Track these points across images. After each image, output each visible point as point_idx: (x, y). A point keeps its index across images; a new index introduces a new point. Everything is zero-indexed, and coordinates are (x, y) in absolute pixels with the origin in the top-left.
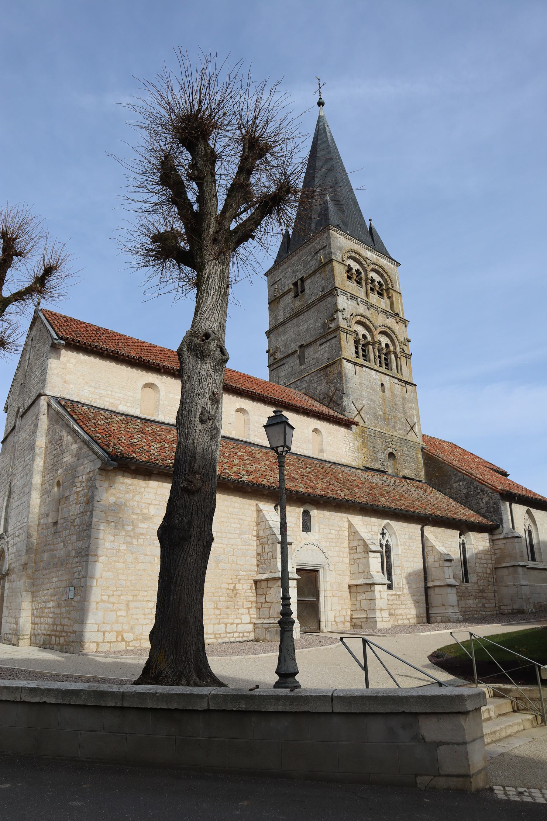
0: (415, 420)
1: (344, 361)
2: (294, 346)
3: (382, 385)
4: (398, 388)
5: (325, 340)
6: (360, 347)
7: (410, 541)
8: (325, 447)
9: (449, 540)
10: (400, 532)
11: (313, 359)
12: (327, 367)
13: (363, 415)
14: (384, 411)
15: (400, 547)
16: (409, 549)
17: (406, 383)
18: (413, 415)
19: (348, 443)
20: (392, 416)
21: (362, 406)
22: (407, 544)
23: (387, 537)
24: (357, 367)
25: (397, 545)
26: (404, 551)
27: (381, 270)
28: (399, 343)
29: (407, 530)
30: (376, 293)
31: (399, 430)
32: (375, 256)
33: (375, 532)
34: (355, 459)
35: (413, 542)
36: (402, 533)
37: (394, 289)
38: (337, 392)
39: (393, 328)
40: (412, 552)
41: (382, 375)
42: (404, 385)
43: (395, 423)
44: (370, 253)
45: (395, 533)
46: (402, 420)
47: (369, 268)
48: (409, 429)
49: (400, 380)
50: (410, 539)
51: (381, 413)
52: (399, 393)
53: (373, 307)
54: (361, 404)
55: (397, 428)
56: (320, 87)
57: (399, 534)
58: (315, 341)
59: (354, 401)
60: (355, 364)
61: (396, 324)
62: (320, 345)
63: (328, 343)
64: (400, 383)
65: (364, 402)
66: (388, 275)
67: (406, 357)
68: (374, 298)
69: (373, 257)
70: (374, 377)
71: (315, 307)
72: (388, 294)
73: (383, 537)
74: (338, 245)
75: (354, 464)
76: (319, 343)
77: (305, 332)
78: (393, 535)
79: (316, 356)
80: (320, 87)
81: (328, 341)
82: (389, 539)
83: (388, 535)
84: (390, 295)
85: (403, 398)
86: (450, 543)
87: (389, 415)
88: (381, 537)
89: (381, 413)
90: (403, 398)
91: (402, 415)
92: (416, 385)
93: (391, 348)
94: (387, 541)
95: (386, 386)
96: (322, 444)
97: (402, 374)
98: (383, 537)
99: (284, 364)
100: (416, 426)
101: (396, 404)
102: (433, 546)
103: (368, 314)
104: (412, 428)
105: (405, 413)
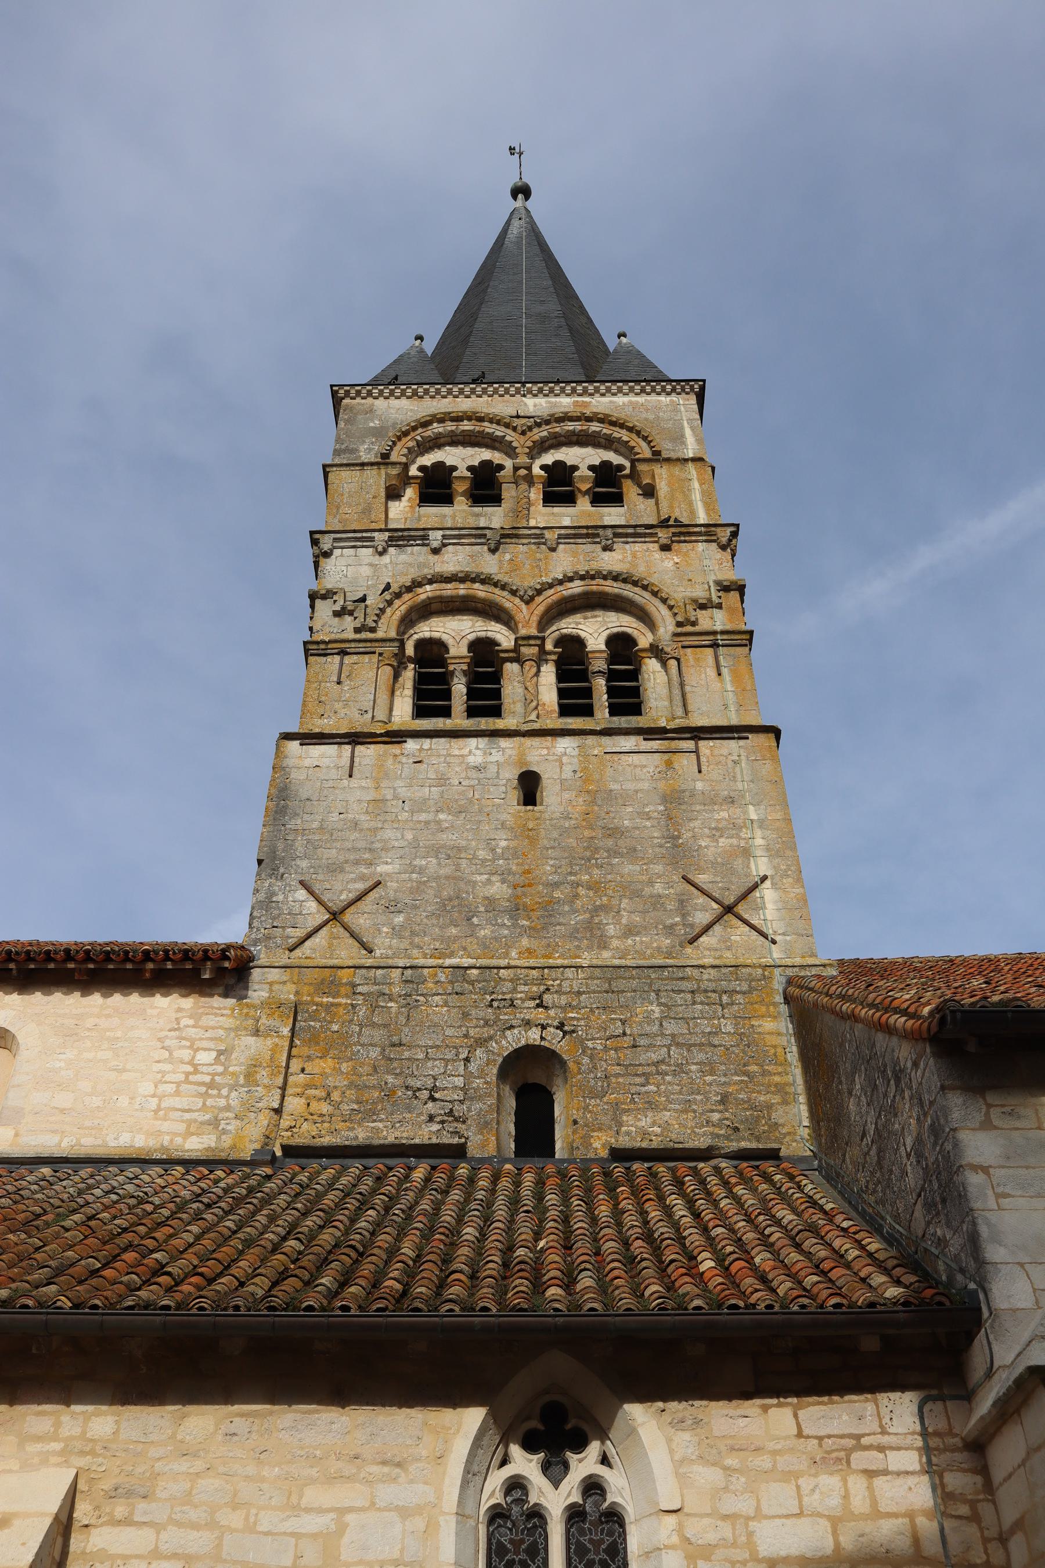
1: (294, 745)
9: (313, 1496)
19: (186, 1054)
27: (595, 427)
28: (671, 608)
34: (215, 1123)
37: (665, 454)
39: (639, 571)
43: (597, 910)
54: (362, 878)
55: (611, 930)
61: (658, 555)
64: (655, 745)
70: (476, 759)
75: (196, 1145)
86: (312, 1523)
87: (556, 885)
89: (498, 889)
101: (614, 832)
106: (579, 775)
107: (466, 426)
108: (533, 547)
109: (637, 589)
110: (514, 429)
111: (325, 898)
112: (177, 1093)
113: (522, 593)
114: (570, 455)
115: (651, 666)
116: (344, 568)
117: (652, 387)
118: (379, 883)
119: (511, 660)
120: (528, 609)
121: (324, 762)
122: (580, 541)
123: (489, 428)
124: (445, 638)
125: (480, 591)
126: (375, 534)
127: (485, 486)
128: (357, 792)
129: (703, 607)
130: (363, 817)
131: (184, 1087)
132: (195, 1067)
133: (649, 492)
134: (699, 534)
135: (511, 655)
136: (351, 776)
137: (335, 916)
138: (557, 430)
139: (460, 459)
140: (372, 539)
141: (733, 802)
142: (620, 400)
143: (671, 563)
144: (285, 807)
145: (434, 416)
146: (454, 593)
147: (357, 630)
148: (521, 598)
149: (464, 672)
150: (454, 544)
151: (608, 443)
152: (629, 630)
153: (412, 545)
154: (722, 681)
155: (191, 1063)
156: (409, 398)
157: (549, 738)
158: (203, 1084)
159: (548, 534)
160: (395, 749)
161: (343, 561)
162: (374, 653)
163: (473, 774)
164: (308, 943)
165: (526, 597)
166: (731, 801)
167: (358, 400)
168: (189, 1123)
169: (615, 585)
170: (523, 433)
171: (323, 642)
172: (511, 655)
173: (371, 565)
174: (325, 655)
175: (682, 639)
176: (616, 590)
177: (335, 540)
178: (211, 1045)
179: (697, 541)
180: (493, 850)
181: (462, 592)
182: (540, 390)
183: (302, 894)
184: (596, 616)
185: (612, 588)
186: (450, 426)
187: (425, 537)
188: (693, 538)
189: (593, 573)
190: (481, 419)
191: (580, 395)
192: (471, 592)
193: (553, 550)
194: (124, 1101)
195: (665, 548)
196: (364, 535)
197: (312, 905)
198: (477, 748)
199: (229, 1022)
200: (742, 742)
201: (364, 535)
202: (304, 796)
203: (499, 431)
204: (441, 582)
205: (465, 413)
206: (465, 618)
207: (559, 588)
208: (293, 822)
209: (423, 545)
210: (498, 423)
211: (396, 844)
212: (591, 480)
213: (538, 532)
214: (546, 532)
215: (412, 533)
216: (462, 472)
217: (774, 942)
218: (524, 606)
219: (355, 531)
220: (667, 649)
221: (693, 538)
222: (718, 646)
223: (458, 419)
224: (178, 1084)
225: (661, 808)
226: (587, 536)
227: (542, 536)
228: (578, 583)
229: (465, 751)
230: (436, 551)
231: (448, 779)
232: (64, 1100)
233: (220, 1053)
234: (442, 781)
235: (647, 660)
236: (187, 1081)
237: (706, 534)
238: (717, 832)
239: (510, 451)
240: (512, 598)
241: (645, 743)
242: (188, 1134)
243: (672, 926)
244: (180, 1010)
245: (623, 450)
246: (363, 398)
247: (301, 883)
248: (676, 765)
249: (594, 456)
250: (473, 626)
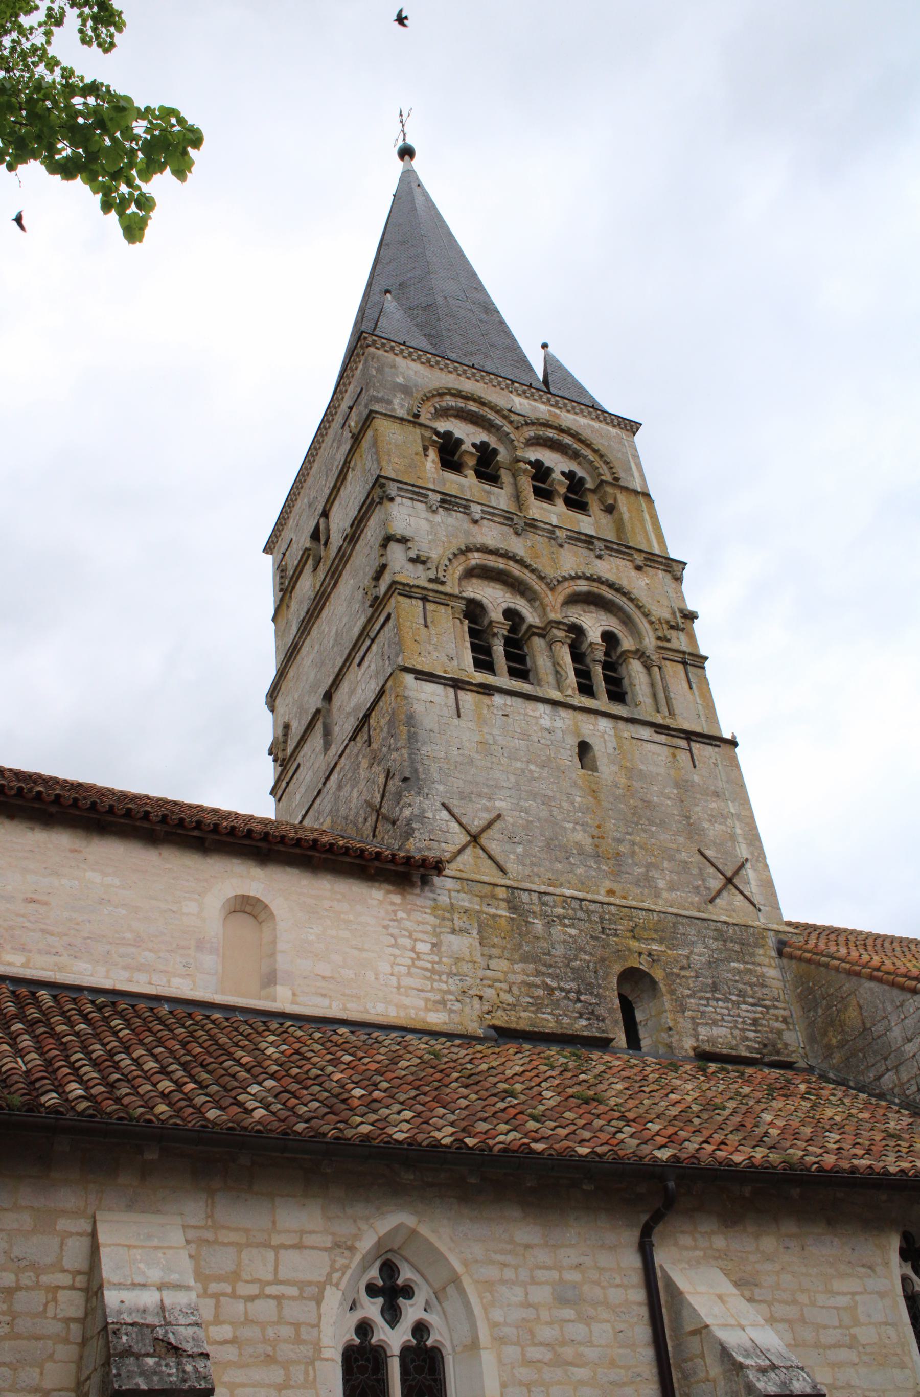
0: (743, 851)
1: (409, 678)
2: (315, 702)
3: (584, 748)
4: (654, 755)
5: (368, 642)
6: (499, 649)
7: (568, 1313)
8: (282, 963)
9: (837, 1285)
10: (492, 1272)
11: (349, 714)
12: (367, 716)
13: (494, 847)
14: (596, 832)
15: (488, 1357)
16: (559, 1362)
17: (690, 736)
18: (733, 837)
19: (408, 942)
20: (633, 844)
21: (487, 817)
22: (547, 1333)
23: (412, 1311)
24: (467, 698)
25: (474, 1346)
26: (524, 1373)
27: (568, 440)
28: (651, 623)
29: (542, 1256)
30: (560, 502)
32: (542, 407)
33: (302, 1285)
34: (443, 1003)
35: (587, 1320)
36: (509, 1274)
37: (622, 483)
38: (390, 782)
39: (624, 583)
40: (581, 1373)
41: (581, 717)
42: (683, 743)
43: (649, 866)
44: (525, 401)
45: (456, 1280)
46: (684, 856)
47: (519, 437)
48: (715, 883)
49: (660, 728)
50: (562, 1301)
51: (580, 836)
52: (662, 770)
53: (535, 527)
54: (487, 809)
55: (661, 884)
56: (403, 125)
57: (489, 1285)
58: (349, 659)
59: (454, 803)
60: (457, 684)
61: (633, 573)
62: (359, 665)
63: (374, 647)
64: (662, 738)
65: (498, 804)
66: (595, 451)
67: (684, 663)
68: (555, 513)
69: (534, 409)
70: (546, 722)
71: (348, 566)
72: (601, 501)
73: (392, 1315)
74: (400, 380)
75: (436, 1019)
77: (333, 646)
78: (451, 1290)
80: (403, 125)
81: (373, 641)
82: (433, 1319)
83: (422, 1294)
84: (610, 502)
85: (683, 786)
86: (842, 1301)
87: (620, 841)
88: (372, 1309)
89: (580, 836)
90: (683, 786)
91: (681, 840)
92: (733, 743)
93: (627, 644)
94: (421, 1329)
95: (602, 749)
96: (273, 955)
97: (672, 713)
98: (392, 1315)
99: (299, 766)
100: (750, 872)
101: (648, 804)
102: (703, 1330)
103: (518, 546)
104: (729, 881)
105: (692, 829)
106: (618, 752)
107: (473, 407)
108: (547, 540)
109: (624, 599)
110: (511, 422)
111: (464, 821)
112: (409, 974)
113: (549, 581)
114: (549, 458)
115: (636, 667)
116: (407, 517)
117: (605, 417)
118: (499, 816)
119: (539, 635)
120: (553, 595)
121: (436, 699)
122: (579, 544)
123: (491, 415)
124: (485, 601)
125: (516, 570)
126: (430, 493)
127: (487, 467)
128: (465, 733)
129: (672, 627)
130: (477, 756)
131: (413, 970)
132: (417, 953)
133: (610, 509)
134: (661, 563)
135: (540, 631)
136: (459, 716)
137: (475, 839)
138: (541, 433)
139: (469, 435)
140: (426, 496)
141: (718, 796)
142: (582, 421)
143: (643, 584)
144: (415, 733)
145: (449, 389)
146: (496, 565)
147: (431, 580)
148: (548, 584)
149: (504, 636)
150: (488, 519)
151: (575, 456)
152: (616, 631)
153: (456, 511)
154: (693, 694)
155: (413, 949)
156: (423, 363)
157: (593, 716)
158: (426, 969)
159: (558, 533)
160: (486, 700)
161: (404, 510)
162: (448, 605)
163: (546, 734)
164: (459, 859)
165: (552, 585)
166: (716, 794)
167: (381, 352)
168: (427, 1000)
169: (609, 591)
170: (517, 428)
171: (408, 585)
172: (540, 631)
173: (427, 520)
174: (411, 597)
175: (663, 651)
176: (610, 597)
177: (399, 489)
178: (425, 937)
179: (658, 569)
180: (572, 803)
181: (501, 566)
182: (524, 392)
183: (445, 814)
184: (591, 612)
185: (609, 594)
186: (460, 403)
187: (466, 507)
188: (656, 566)
189: (595, 577)
190: (483, 404)
191: (552, 406)
192: (508, 568)
193: (561, 546)
194: (371, 976)
195: (638, 568)
196: (421, 491)
197: (455, 826)
198: (545, 713)
199: (431, 919)
200: (716, 749)
201: (421, 491)
202: (428, 728)
203: (499, 421)
204: (485, 552)
205: (490, 402)
206: (498, 586)
207: (572, 583)
208: (424, 749)
209: (465, 513)
210: (497, 412)
211: (505, 785)
212: (566, 486)
213: (550, 528)
214: (556, 529)
215: (458, 501)
216: (467, 446)
217: (760, 910)
218: (549, 593)
219: (413, 485)
220: (653, 658)
221: (656, 566)
222: (687, 663)
223: (466, 398)
224: (409, 967)
225: (675, 792)
226: (585, 542)
227: (553, 532)
228: (582, 582)
229: (537, 714)
230: (475, 522)
231: (530, 735)
232: (324, 969)
233: (434, 945)
234: (525, 736)
235: (631, 660)
236: (413, 965)
237: (666, 565)
238: (712, 819)
239: (504, 438)
240: (540, 583)
241: (655, 735)
242: (427, 1010)
243: (697, 888)
244: (393, 904)
245: (586, 465)
246: (386, 351)
247: (443, 804)
248: (678, 758)
249: (573, 466)
250: (504, 597)
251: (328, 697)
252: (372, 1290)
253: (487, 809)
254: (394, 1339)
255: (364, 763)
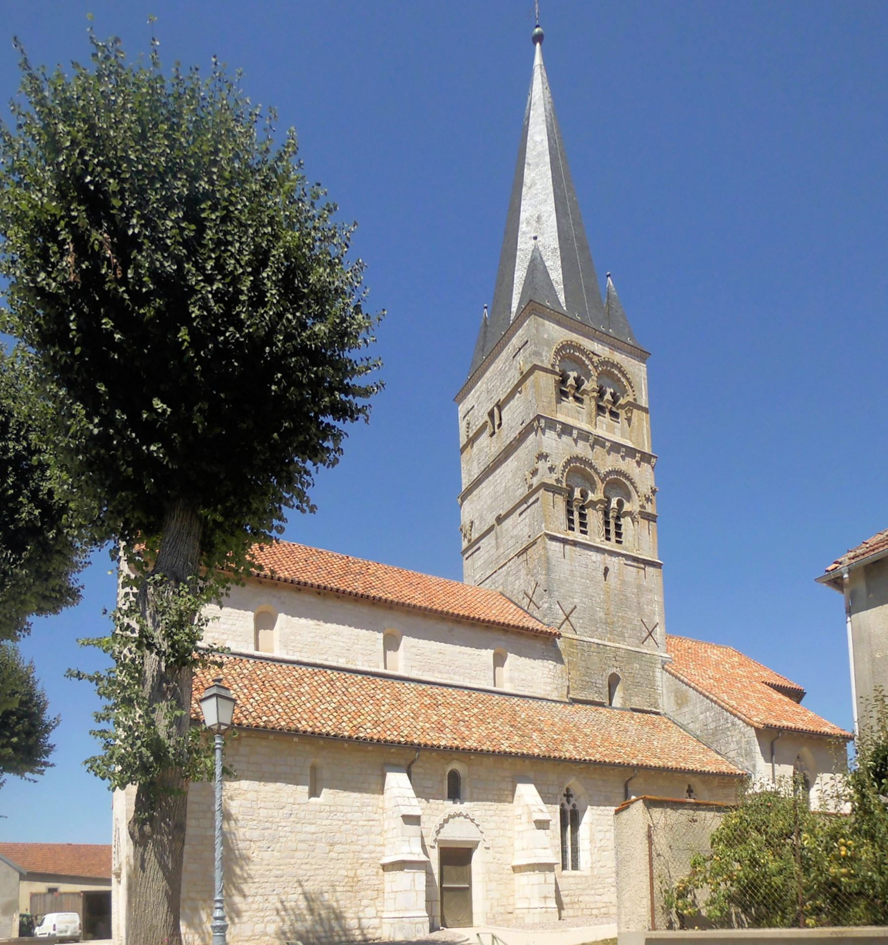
11: (512, 537)
12: (525, 550)
20: (618, 616)
23: (573, 801)
31: (630, 637)
42: (642, 566)
46: (636, 622)
51: (602, 615)
52: (632, 580)
54: (571, 603)
59: (561, 601)
65: (575, 600)
73: (568, 802)
76: (518, 511)
79: (515, 533)
85: (639, 587)
90: (639, 587)
94: (574, 806)
98: (568, 802)
105: (640, 608)
251: (500, 520)
252: (565, 795)
253: (571, 603)
254: (569, 807)
255: (523, 572)
